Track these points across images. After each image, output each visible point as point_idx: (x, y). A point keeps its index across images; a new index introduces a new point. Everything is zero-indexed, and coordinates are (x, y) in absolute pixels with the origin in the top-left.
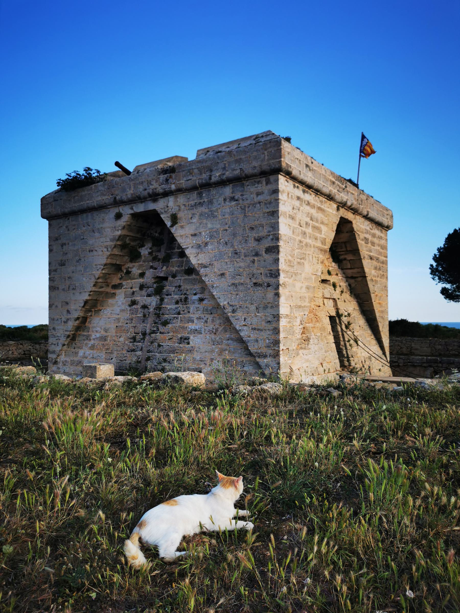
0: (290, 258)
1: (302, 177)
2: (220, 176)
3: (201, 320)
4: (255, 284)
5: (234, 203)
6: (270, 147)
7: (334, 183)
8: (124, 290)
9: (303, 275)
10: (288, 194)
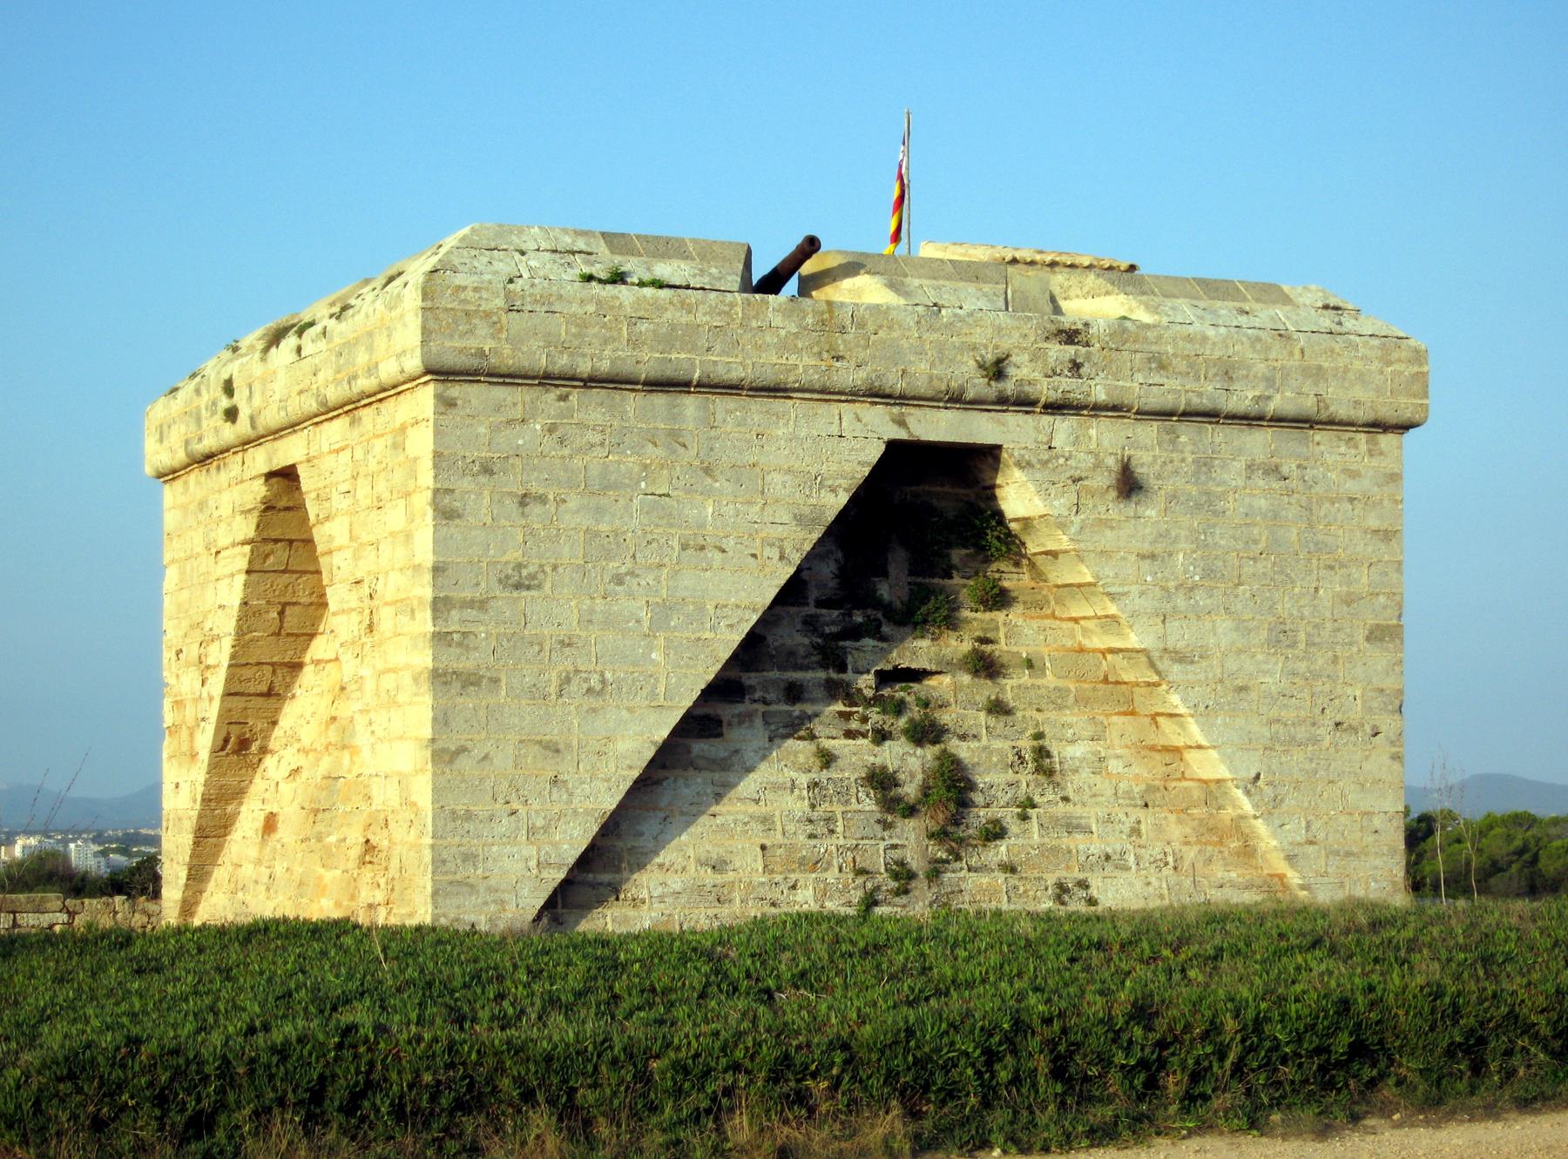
2: (1257, 399)
3: (1118, 827)
4: (1337, 724)
5: (1276, 485)
6: (1399, 360)
8: (761, 708)
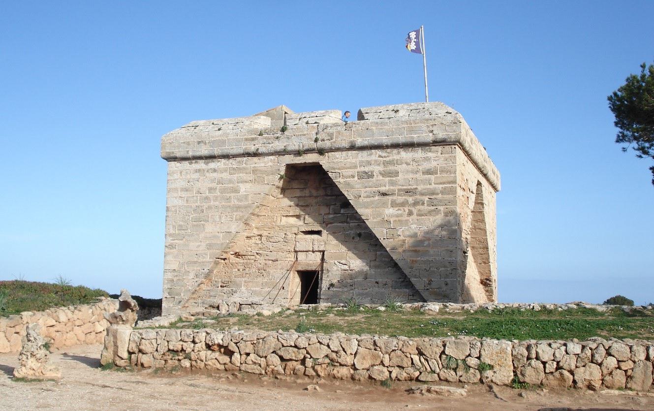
0: (181, 223)
1: (190, 154)
7: (253, 139)
9: (202, 235)
10: (181, 173)
